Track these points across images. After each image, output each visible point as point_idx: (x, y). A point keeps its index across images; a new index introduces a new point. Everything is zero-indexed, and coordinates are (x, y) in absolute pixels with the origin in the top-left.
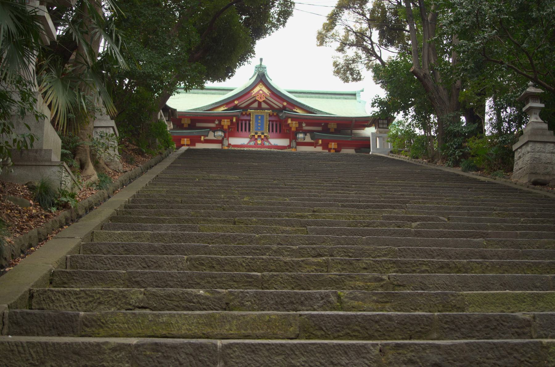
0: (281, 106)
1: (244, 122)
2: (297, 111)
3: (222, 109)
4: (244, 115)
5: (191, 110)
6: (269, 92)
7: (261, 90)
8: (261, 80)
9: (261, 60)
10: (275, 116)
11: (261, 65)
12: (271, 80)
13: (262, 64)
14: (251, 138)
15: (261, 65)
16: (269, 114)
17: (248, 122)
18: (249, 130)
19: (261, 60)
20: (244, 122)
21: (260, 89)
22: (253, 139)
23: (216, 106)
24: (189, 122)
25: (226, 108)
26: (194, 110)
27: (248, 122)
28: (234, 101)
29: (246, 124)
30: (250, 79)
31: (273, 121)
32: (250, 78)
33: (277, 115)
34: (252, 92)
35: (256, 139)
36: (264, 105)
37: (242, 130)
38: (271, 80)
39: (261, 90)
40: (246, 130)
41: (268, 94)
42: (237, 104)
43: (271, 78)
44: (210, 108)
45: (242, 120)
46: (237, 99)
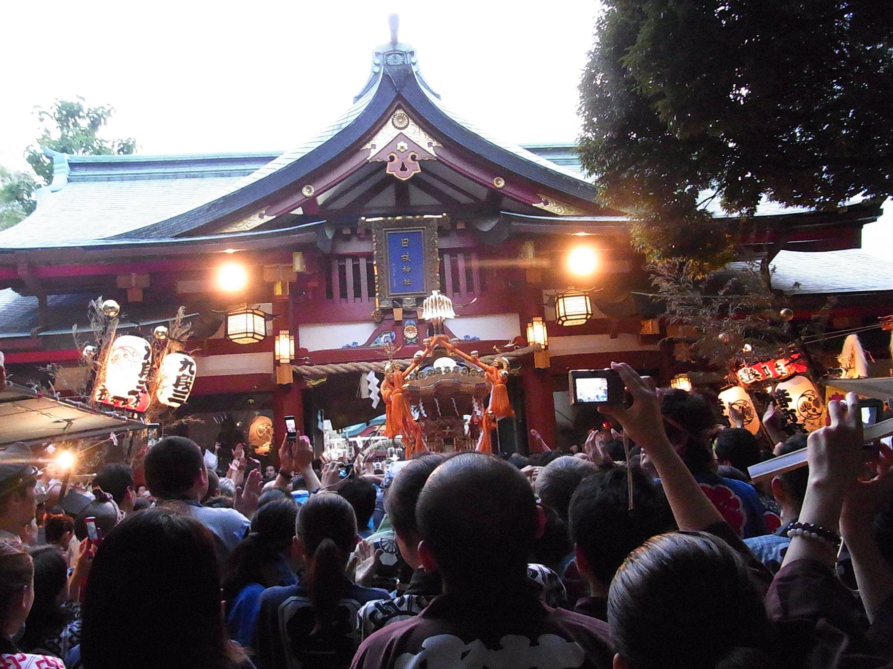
0: (483, 193)
1: (349, 263)
2: (546, 208)
3: (255, 221)
4: (347, 238)
5: (127, 235)
6: (435, 144)
7: (401, 137)
8: (399, 97)
9: (394, 22)
10: (460, 233)
11: (394, 43)
12: (438, 96)
13: (399, 40)
14: (377, 323)
15: (394, 43)
16: (440, 229)
17: (363, 262)
18: (372, 294)
19: (394, 22)
20: (349, 263)
21: (399, 131)
22: (386, 324)
23: (227, 211)
24: (144, 280)
25: (267, 218)
26: (137, 233)
27: (363, 262)
28: (296, 187)
29: (356, 268)
30: (358, 98)
31: (453, 252)
32: (357, 94)
33: (471, 231)
34: (368, 146)
35: (399, 323)
36: (418, 197)
37: (344, 295)
38: (438, 96)
39: (401, 137)
40: (358, 293)
41: (431, 150)
42: (313, 199)
43: (437, 92)
44: (201, 222)
45: (344, 257)
46: (312, 178)
